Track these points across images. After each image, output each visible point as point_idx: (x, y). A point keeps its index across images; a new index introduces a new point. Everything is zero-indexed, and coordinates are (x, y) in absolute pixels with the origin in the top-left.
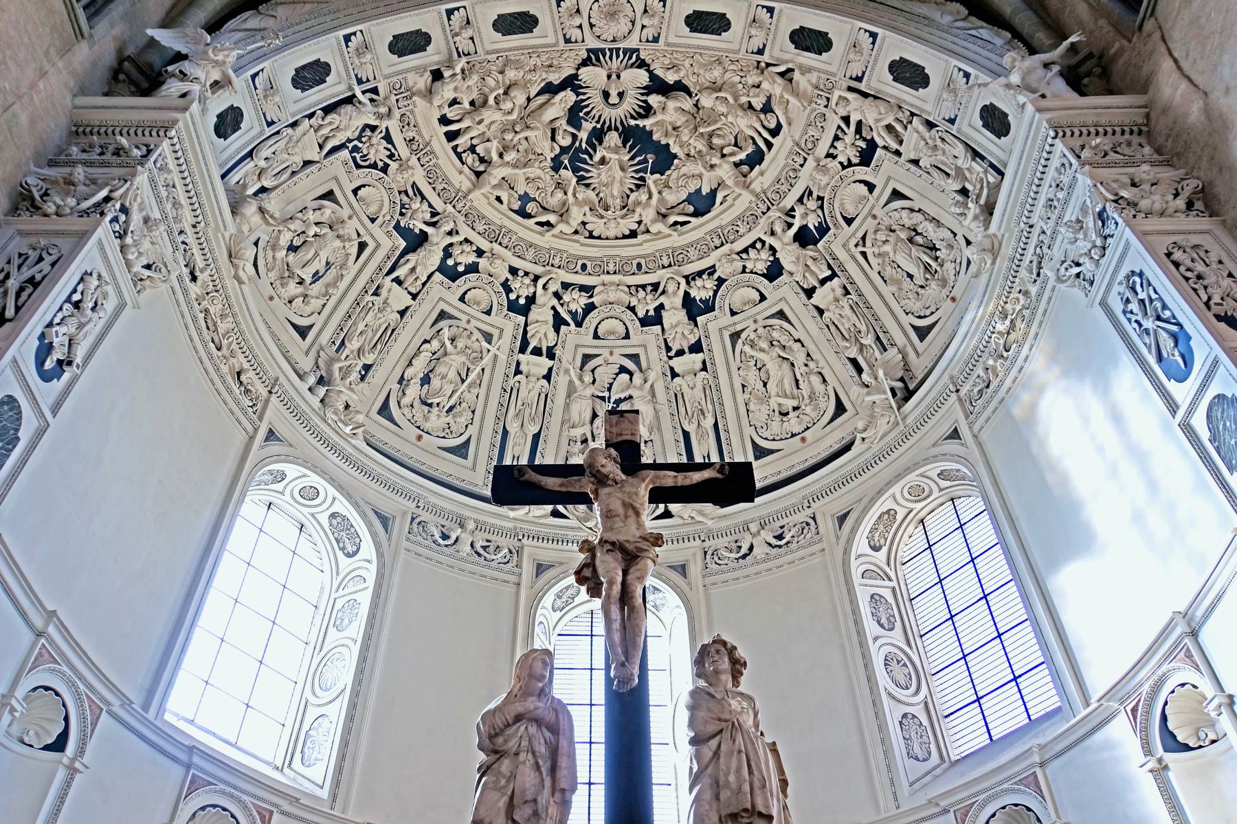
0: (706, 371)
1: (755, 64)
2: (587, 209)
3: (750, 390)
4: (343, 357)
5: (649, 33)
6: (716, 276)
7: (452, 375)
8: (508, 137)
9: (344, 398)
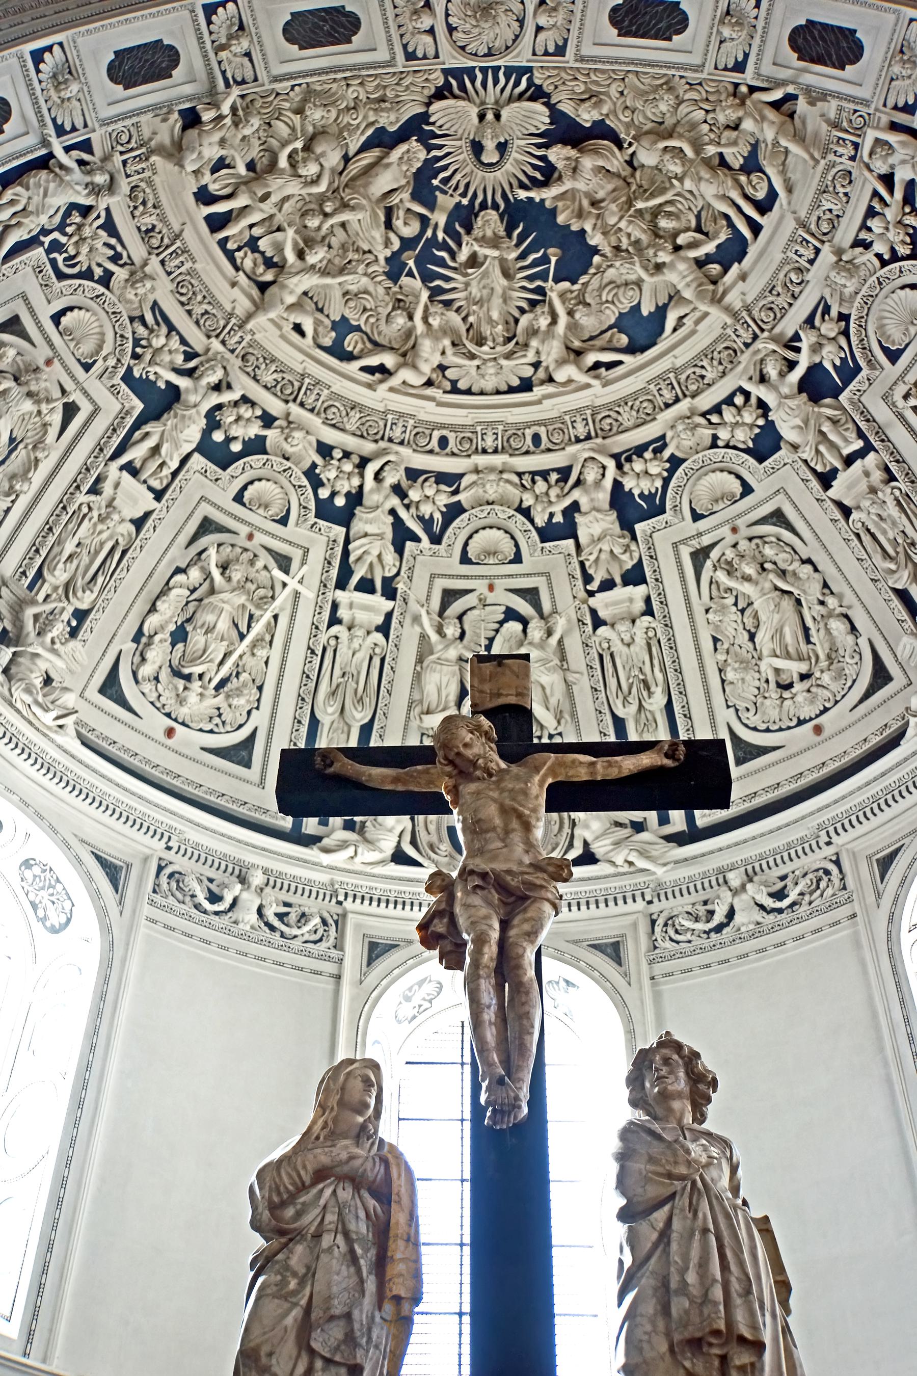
0: (652, 614)
1: (731, 88)
2: (447, 342)
3: (726, 646)
4: (41, 597)
5: (549, 39)
6: (666, 454)
7: (223, 625)
8: (313, 222)
9: (43, 665)
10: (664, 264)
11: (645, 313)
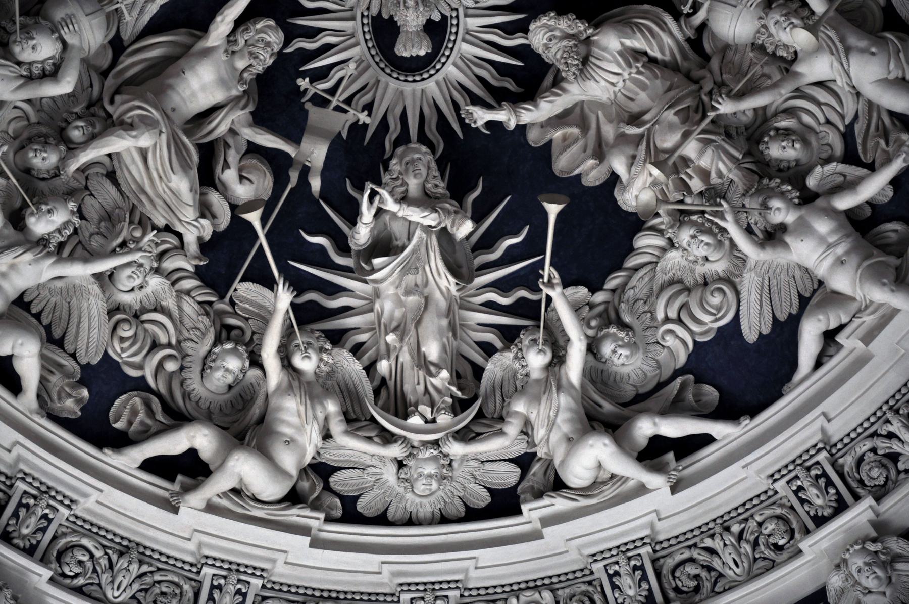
2: (332, 407)
10: (783, 228)
11: (750, 335)
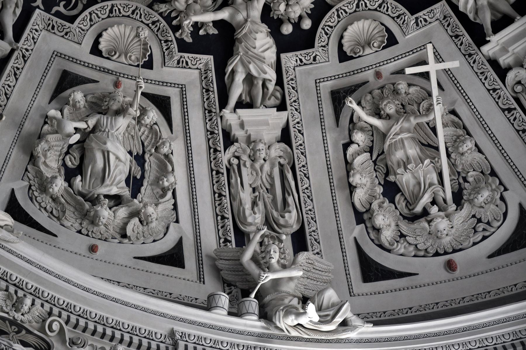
7: (413, 151)
